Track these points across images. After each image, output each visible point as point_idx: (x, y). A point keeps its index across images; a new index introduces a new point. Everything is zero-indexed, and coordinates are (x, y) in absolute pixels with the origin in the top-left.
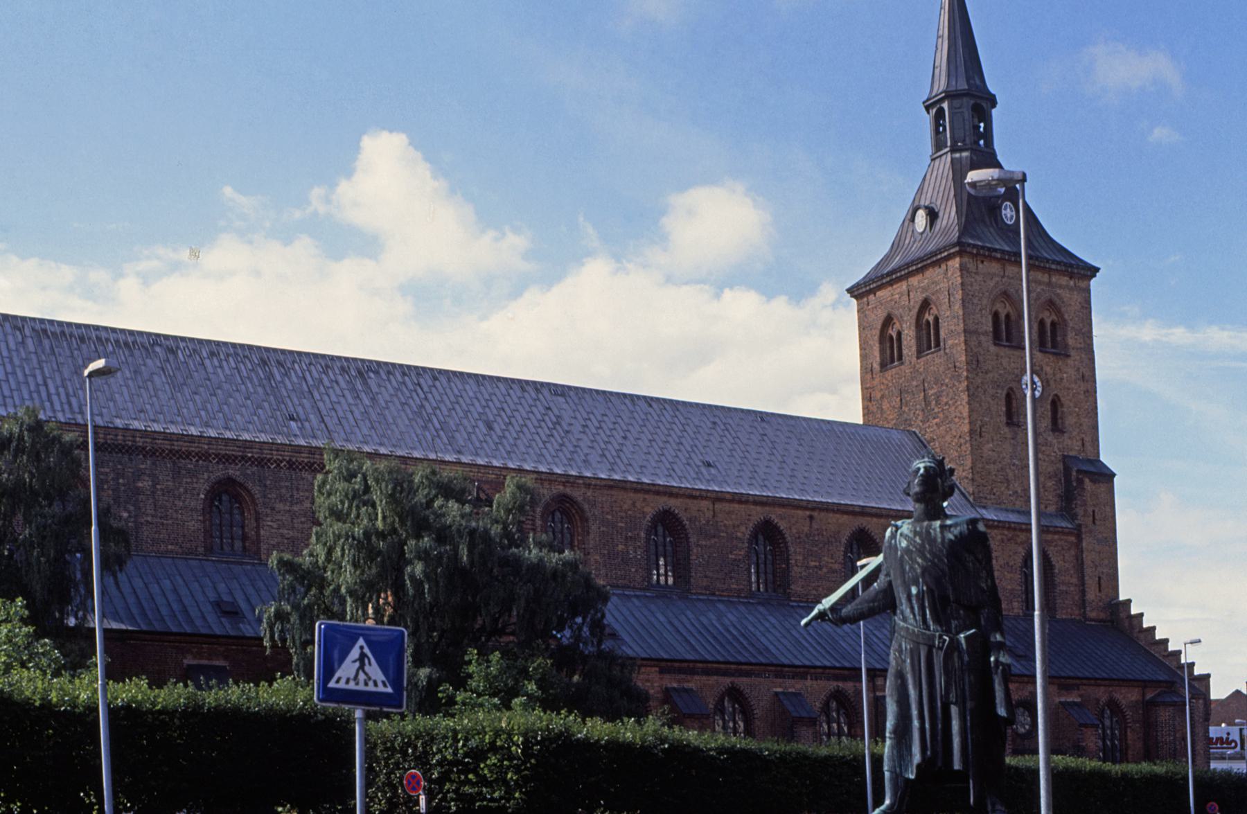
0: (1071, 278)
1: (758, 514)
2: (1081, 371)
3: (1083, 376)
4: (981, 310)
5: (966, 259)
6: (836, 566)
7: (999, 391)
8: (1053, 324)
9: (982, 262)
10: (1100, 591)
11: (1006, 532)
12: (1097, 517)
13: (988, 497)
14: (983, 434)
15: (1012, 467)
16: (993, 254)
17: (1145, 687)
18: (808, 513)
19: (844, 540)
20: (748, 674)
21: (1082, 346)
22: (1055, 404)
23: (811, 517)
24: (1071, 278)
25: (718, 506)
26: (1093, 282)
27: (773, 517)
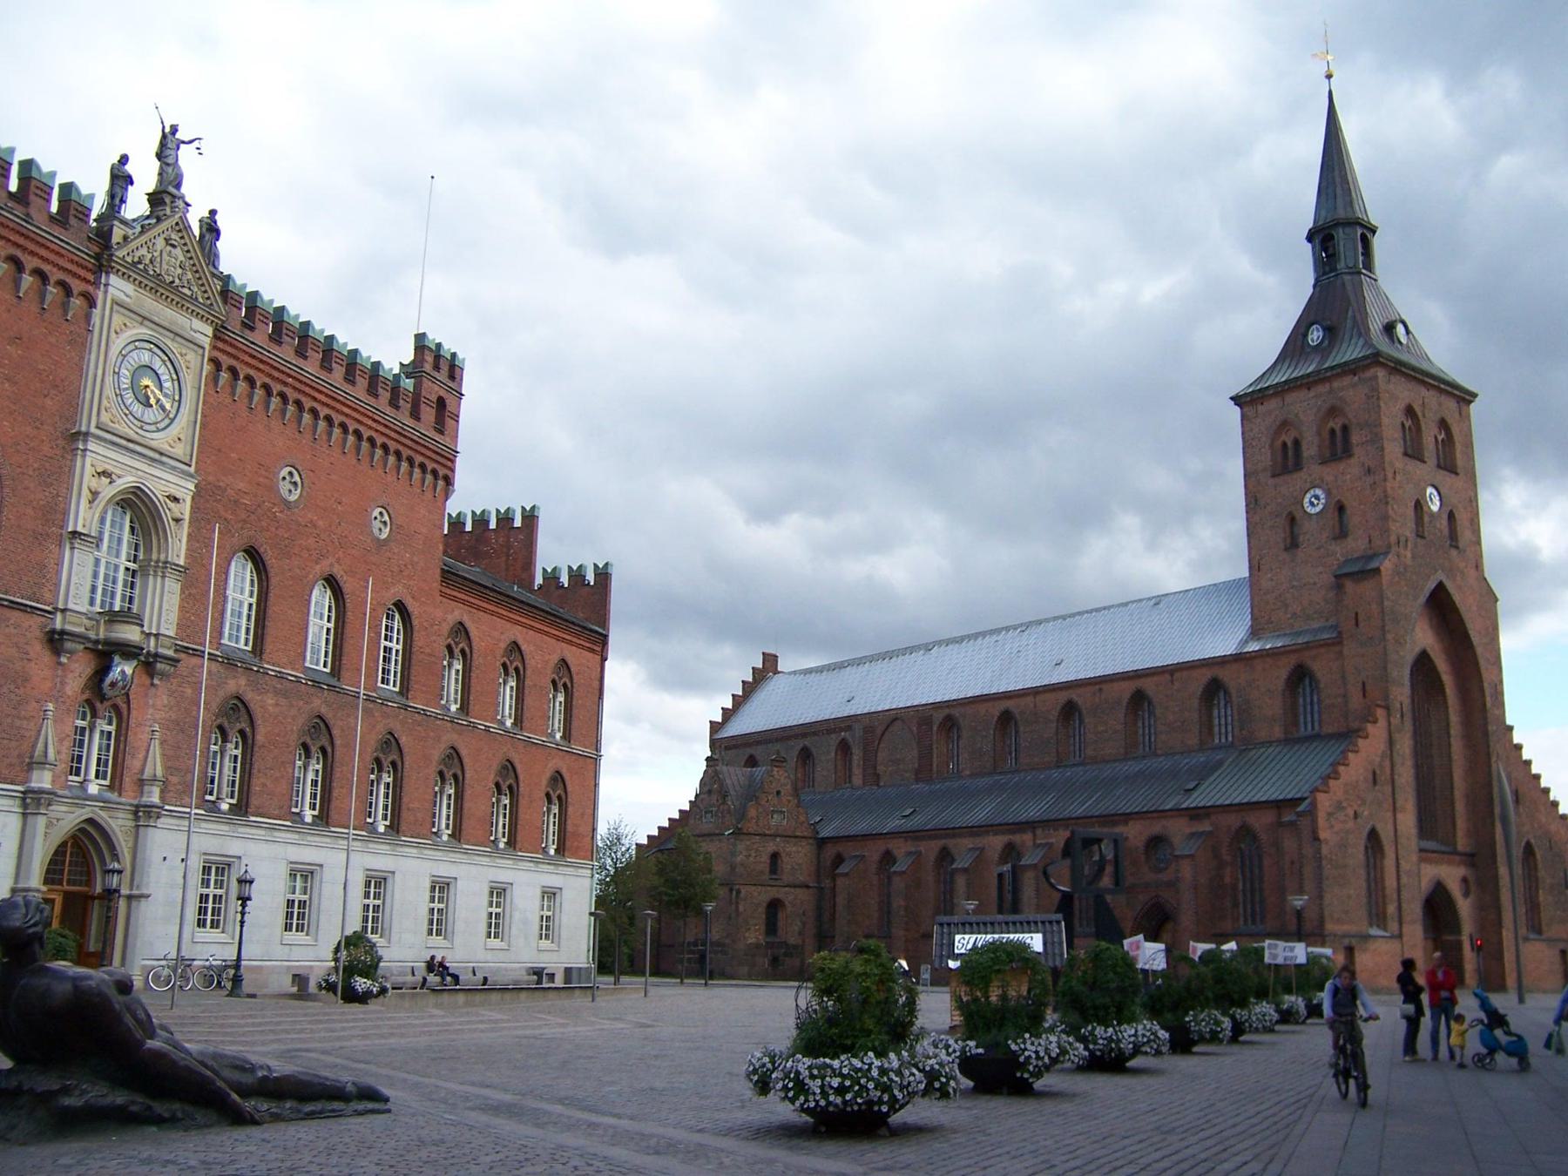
1: (1063, 697)
7: (1278, 520)
10: (1364, 696)
12: (1360, 619)
16: (1267, 393)
17: (1034, 828)
18: (1097, 687)
19: (1125, 704)
20: (954, 836)
22: (1341, 508)
23: (1100, 689)
24: (1355, 375)
25: (1038, 698)
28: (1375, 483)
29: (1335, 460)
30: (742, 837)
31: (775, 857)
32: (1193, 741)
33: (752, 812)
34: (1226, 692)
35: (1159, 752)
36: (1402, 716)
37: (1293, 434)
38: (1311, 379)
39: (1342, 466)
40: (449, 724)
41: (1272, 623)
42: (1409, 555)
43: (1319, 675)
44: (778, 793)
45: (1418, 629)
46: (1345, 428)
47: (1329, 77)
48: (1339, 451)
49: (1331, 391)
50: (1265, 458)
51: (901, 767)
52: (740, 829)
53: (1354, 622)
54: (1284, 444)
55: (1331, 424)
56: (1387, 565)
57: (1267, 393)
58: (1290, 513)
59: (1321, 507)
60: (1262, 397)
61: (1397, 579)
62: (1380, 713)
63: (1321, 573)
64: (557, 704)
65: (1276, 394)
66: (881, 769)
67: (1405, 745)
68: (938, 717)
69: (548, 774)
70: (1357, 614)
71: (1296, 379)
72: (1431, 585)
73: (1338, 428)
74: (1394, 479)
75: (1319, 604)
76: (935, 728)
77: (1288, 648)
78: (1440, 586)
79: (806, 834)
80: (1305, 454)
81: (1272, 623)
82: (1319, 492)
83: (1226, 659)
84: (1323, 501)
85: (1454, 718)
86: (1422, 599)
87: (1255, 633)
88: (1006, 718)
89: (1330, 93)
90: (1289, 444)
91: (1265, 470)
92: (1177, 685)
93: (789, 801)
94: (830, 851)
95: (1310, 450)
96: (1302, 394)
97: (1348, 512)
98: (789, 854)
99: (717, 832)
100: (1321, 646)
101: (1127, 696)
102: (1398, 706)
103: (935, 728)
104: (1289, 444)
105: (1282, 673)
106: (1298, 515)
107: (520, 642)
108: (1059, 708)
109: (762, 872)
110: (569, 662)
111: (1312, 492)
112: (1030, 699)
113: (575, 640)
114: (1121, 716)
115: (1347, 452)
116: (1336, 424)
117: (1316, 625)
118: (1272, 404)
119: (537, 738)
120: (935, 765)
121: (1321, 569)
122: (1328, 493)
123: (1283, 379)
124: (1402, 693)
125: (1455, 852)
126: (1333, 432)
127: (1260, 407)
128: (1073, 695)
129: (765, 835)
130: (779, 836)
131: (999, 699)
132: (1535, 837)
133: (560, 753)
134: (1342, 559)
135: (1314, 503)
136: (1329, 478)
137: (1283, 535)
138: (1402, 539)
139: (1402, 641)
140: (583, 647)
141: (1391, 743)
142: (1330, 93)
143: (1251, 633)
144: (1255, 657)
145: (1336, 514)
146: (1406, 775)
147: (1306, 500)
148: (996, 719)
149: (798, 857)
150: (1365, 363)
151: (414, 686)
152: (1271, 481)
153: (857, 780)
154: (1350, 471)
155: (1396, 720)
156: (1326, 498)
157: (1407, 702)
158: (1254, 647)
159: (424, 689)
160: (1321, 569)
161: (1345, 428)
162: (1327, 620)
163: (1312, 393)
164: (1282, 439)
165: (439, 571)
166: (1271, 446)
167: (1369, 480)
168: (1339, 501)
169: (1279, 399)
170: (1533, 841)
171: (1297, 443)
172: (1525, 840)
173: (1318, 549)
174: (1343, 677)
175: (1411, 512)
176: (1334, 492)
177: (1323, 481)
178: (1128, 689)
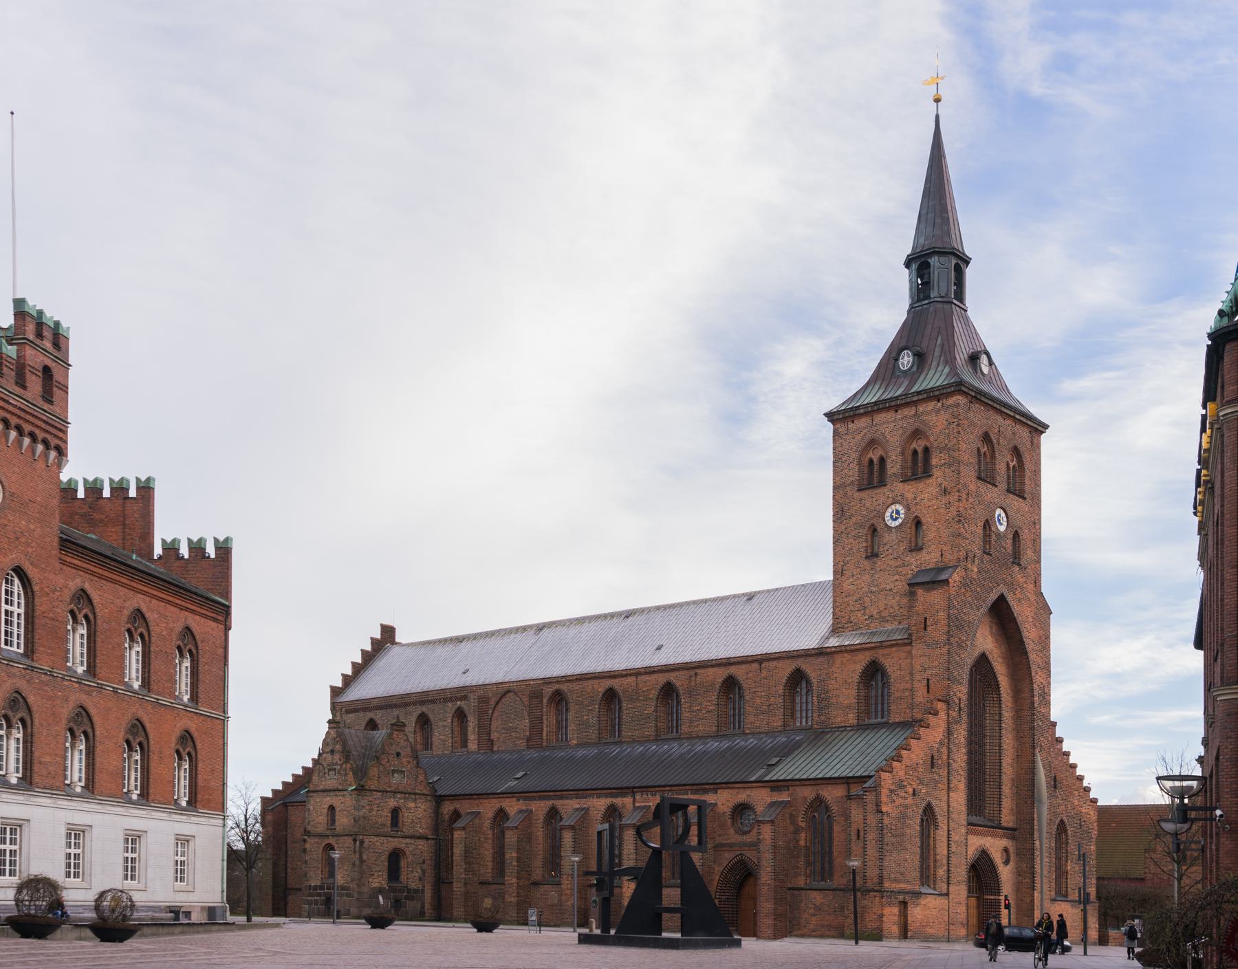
0: (939, 401)
1: (662, 679)
2: (943, 486)
4: (849, 465)
6: (712, 707)
7: (861, 531)
9: (853, 422)
10: (928, 692)
11: (846, 655)
12: (928, 624)
13: (846, 626)
14: (844, 572)
15: (869, 595)
16: (857, 412)
19: (718, 687)
21: (947, 461)
22: (918, 523)
27: (672, 679)
28: (949, 503)
29: (916, 479)
30: (364, 792)
31: (395, 812)
32: (778, 723)
33: (374, 771)
34: (808, 682)
35: (747, 731)
36: (960, 710)
37: (880, 452)
38: (899, 402)
39: (921, 485)
40: (76, 685)
41: (851, 622)
42: (976, 570)
43: (889, 670)
44: (398, 754)
45: (978, 635)
46: (926, 450)
48: (920, 471)
49: (916, 415)
50: (853, 473)
51: (513, 734)
52: (362, 786)
53: (923, 626)
54: (871, 461)
55: (914, 445)
56: (956, 577)
57: (857, 412)
58: (873, 525)
59: (900, 521)
61: (963, 590)
62: (941, 706)
63: (897, 581)
64: (183, 669)
65: (865, 414)
66: (494, 736)
67: (961, 734)
68: (548, 691)
69: (177, 732)
70: (926, 619)
71: (885, 401)
72: (993, 597)
73: (920, 450)
74: (967, 500)
75: (893, 608)
76: (545, 701)
77: (863, 646)
78: (1002, 598)
79: (424, 792)
80: (890, 471)
81: (851, 622)
82: (899, 507)
83: (809, 652)
84: (902, 516)
85: (1007, 714)
86: (984, 609)
87: (835, 630)
88: (611, 696)
90: (875, 461)
91: (852, 483)
92: (764, 672)
93: (409, 762)
94: (447, 808)
95: (894, 467)
96: (890, 415)
97: (924, 527)
98: (408, 809)
99: (340, 787)
100: (893, 646)
101: (720, 680)
102: (957, 701)
103: (545, 701)
104: (875, 461)
105: (858, 665)
106: (880, 527)
107: (144, 610)
108: (658, 687)
109: (384, 825)
110: (194, 630)
111: (893, 507)
112: (631, 680)
113: (199, 610)
114: (714, 698)
115: (927, 473)
116: (918, 445)
117: (889, 627)
118: (862, 423)
119: (165, 701)
120: (544, 733)
121: (897, 577)
122: (908, 508)
123: (873, 400)
124: (961, 691)
125: (999, 827)
126: (915, 452)
127: (851, 425)
128: (672, 677)
129: (387, 792)
130: (401, 793)
131: (604, 677)
132: (1067, 817)
133: (188, 714)
134: (915, 570)
135: (895, 515)
136: (910, 496)
137: (865, 545)
138: (970, 555)
139: (964, 645)
140: (206, 617)
141: (949, 732)
143: (832, 631)
144: (835, 652)
145: (914, 528)
146: (960, 759)
147: (888, 514)
148: (600, 695)
149: (417, 813)
151: (40, 649)
152: (857, 495)
153: (473, 746)
154: (926, 492)
155: (954, 714)
156: (906, 513)
157: (964, 697)
158: (833, 642)
159: (49, 651)
160: (897, 577)
161: (926, 450)
162: (900, 623)
163: (899, 415)
164: (868, 456)
165: (57, 540)
166: (859, 462)
167: (944, 499)
168: (917, 517)
169: (868, 419)
170: (1066, 820)
171: (882, 460)
172: (1059, 819)
174: (911, 674)
175: (979, 530)
176: (913, 508)
177: (903, 498)
178: (721, 674)
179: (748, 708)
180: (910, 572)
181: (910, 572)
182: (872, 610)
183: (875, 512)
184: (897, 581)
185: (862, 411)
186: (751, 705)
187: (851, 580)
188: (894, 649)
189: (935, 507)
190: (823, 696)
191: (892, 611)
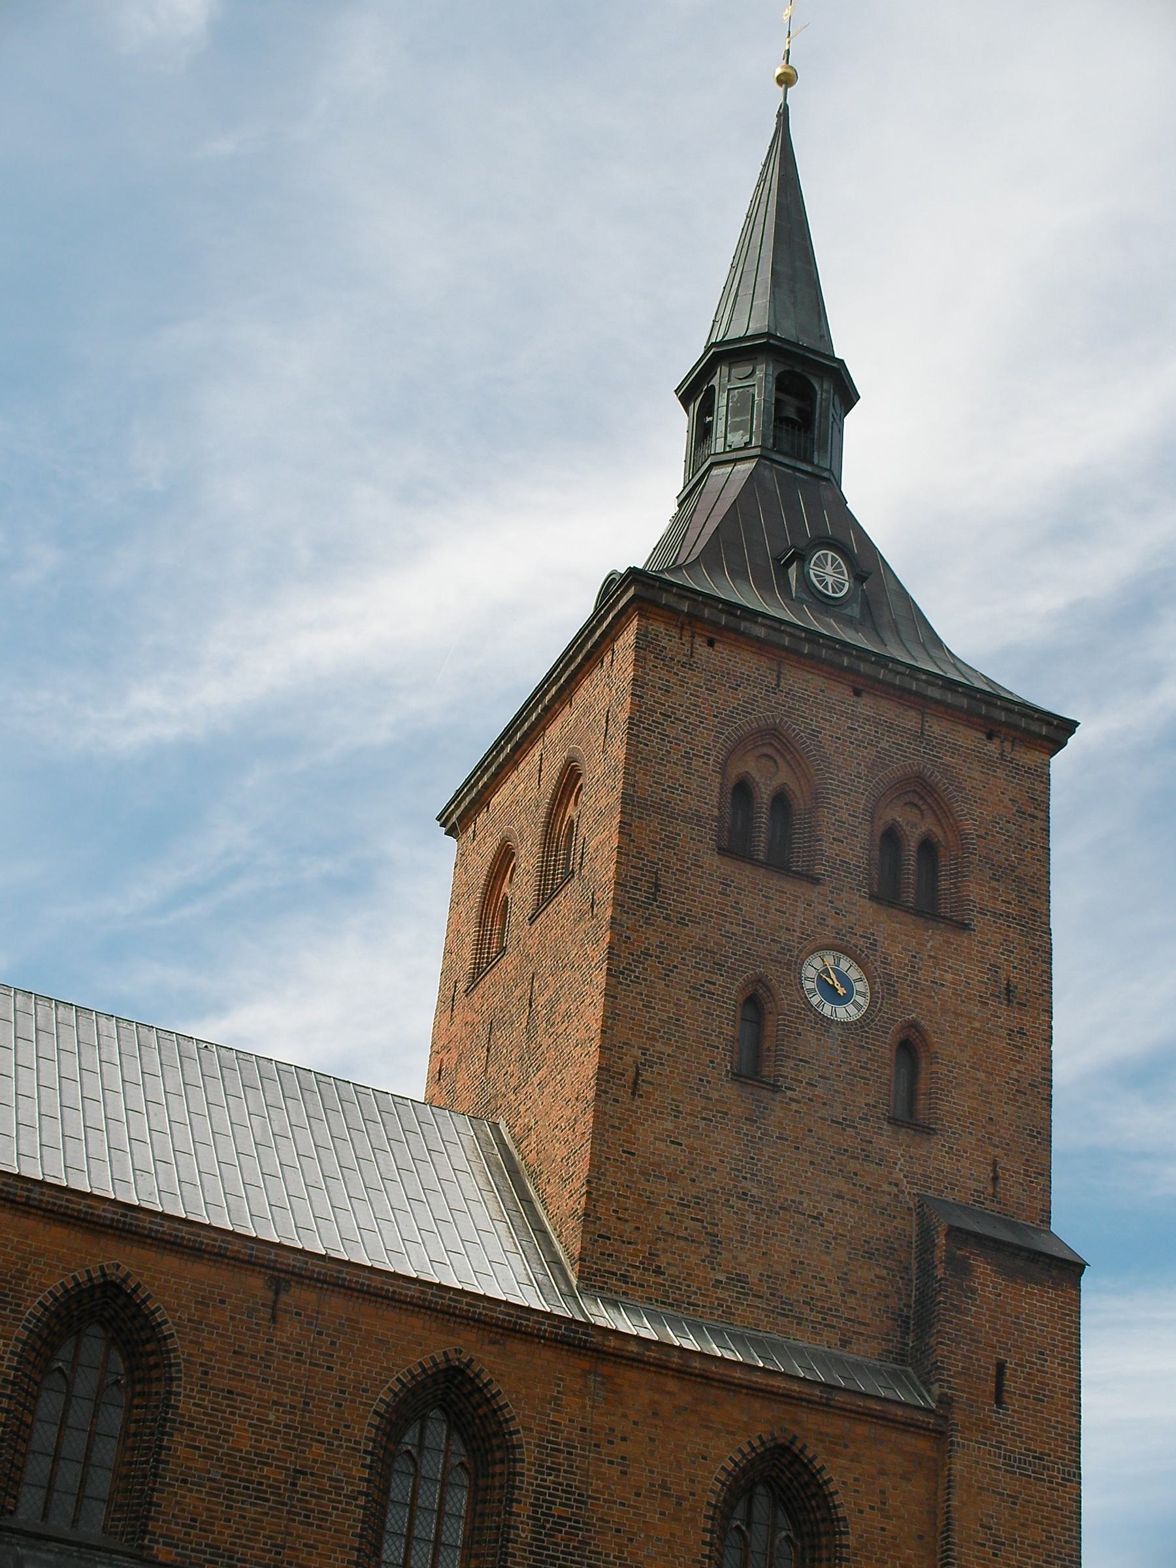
0: (990, 736)
3: (1008, 991)
5: (657, 627)
8: (928, 847)
11: (672, 1385)
12: (1009, 1385)
13: (635, 1276)
19: (31, 1308)
21: (1013, 910)
24: (990, 736)
26: (1060, 763)
43: (845, 1502)
47: (786, 80)
53: (991, 1386)
60: (727, 628)
65: (761, 646)
70: (1001, 1367)
75: (822, 1282)
81: (658, 1271)
83: (529, 1323)
89: (784, 115)
100: (864, 1415)
121: (838, 1184)
127: (703, 650)
142: (784, 115)
144: (634, 1361)
150: (1035, 727)
160: (838, 1184)
162: (845, 1343)
168: (914, 1025)
173: (841, 1124)
179: (181, 1451)
180: (886, 1187)
181: (886, 1187)
182: (743, 1258)
183: (775, 947)
184: (839, 1196)
185: (761, 632)
186: (202, 1441)
187: (669, 1125)
188: (862, 1429)
189: (977, 1025)
190: (557, 1510)
191: (819, 1290)
